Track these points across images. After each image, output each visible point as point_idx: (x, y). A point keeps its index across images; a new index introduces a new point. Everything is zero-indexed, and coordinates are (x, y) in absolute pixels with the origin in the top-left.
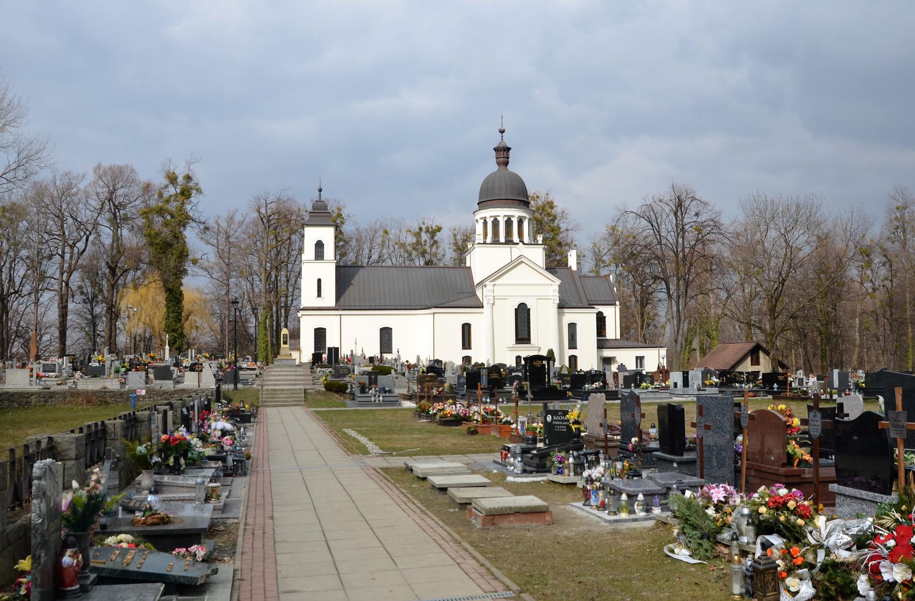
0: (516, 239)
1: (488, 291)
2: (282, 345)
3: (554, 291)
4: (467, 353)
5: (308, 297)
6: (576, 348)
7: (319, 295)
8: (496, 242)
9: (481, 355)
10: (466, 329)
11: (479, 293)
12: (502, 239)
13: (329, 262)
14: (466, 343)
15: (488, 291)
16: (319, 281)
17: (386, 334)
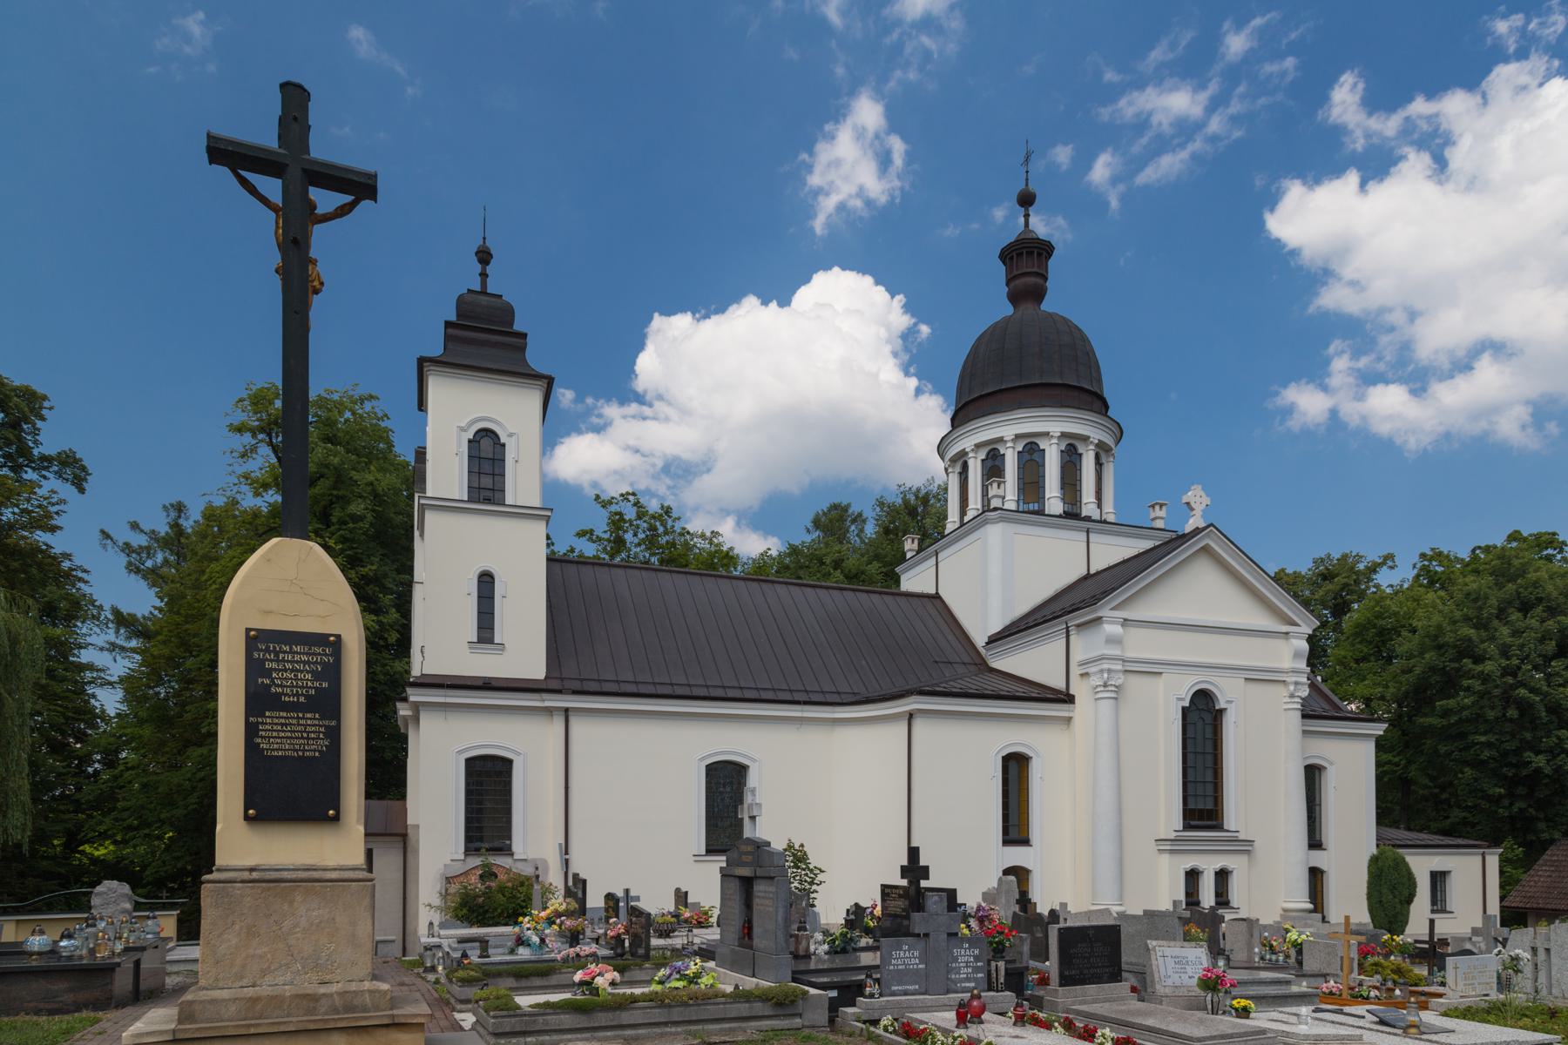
0: (1089, 507)
2: (239, 843)
10: (1015, 767)
12: (1054, 505)
13: (523, 513)
14: (1015, 830)
16: (486, 581)
17: (726, 785)
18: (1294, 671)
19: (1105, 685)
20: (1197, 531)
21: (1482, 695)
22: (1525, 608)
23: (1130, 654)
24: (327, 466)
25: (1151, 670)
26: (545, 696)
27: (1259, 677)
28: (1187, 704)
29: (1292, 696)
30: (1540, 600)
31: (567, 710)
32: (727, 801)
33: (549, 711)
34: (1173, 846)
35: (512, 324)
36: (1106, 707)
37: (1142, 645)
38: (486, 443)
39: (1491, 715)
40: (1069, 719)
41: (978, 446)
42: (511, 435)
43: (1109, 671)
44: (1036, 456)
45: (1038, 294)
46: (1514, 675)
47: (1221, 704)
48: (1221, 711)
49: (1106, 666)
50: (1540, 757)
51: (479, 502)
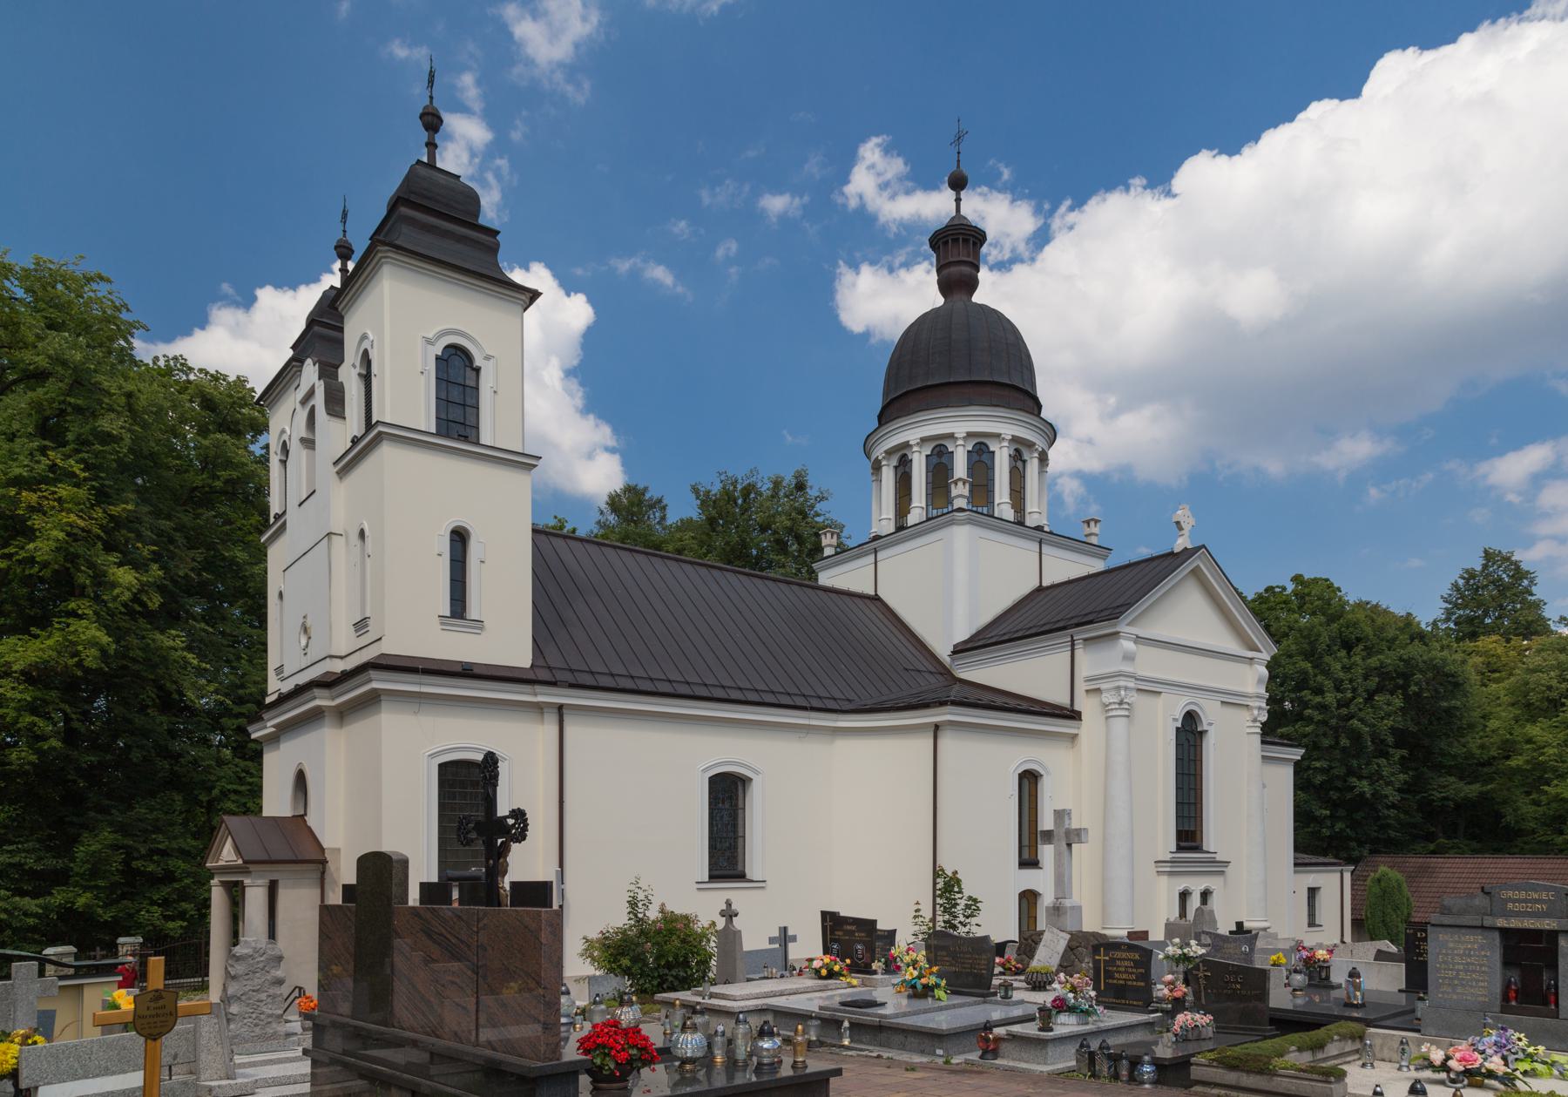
15: (1129, 657)
16: (460, 538)
19: (1121, 703)
20: (1187, 553)
21: (1325, 723)
22: (1348, 646)
23: (1141, 673)
24: (64, 363)
25: (1151, 688)
26: (538, 688)
27: (1232, 701)
29: (1255, 720)
30: (1359, 640)
31: (560, 707)
32: (726, 819)
33: (539, 708)
34: (1171, 868)
35: (477, 216)
36: (1119, 725)
37: (1152, 664)
39: (1326, 742)
40: (1074, 737)
41: (924, 440)
43: (1126, 688)
44: (985, 457)
45: (971, 285)
48: (1202, 733)
49: (1122, 683)
50: (1365, 783)
51: (447, 436)
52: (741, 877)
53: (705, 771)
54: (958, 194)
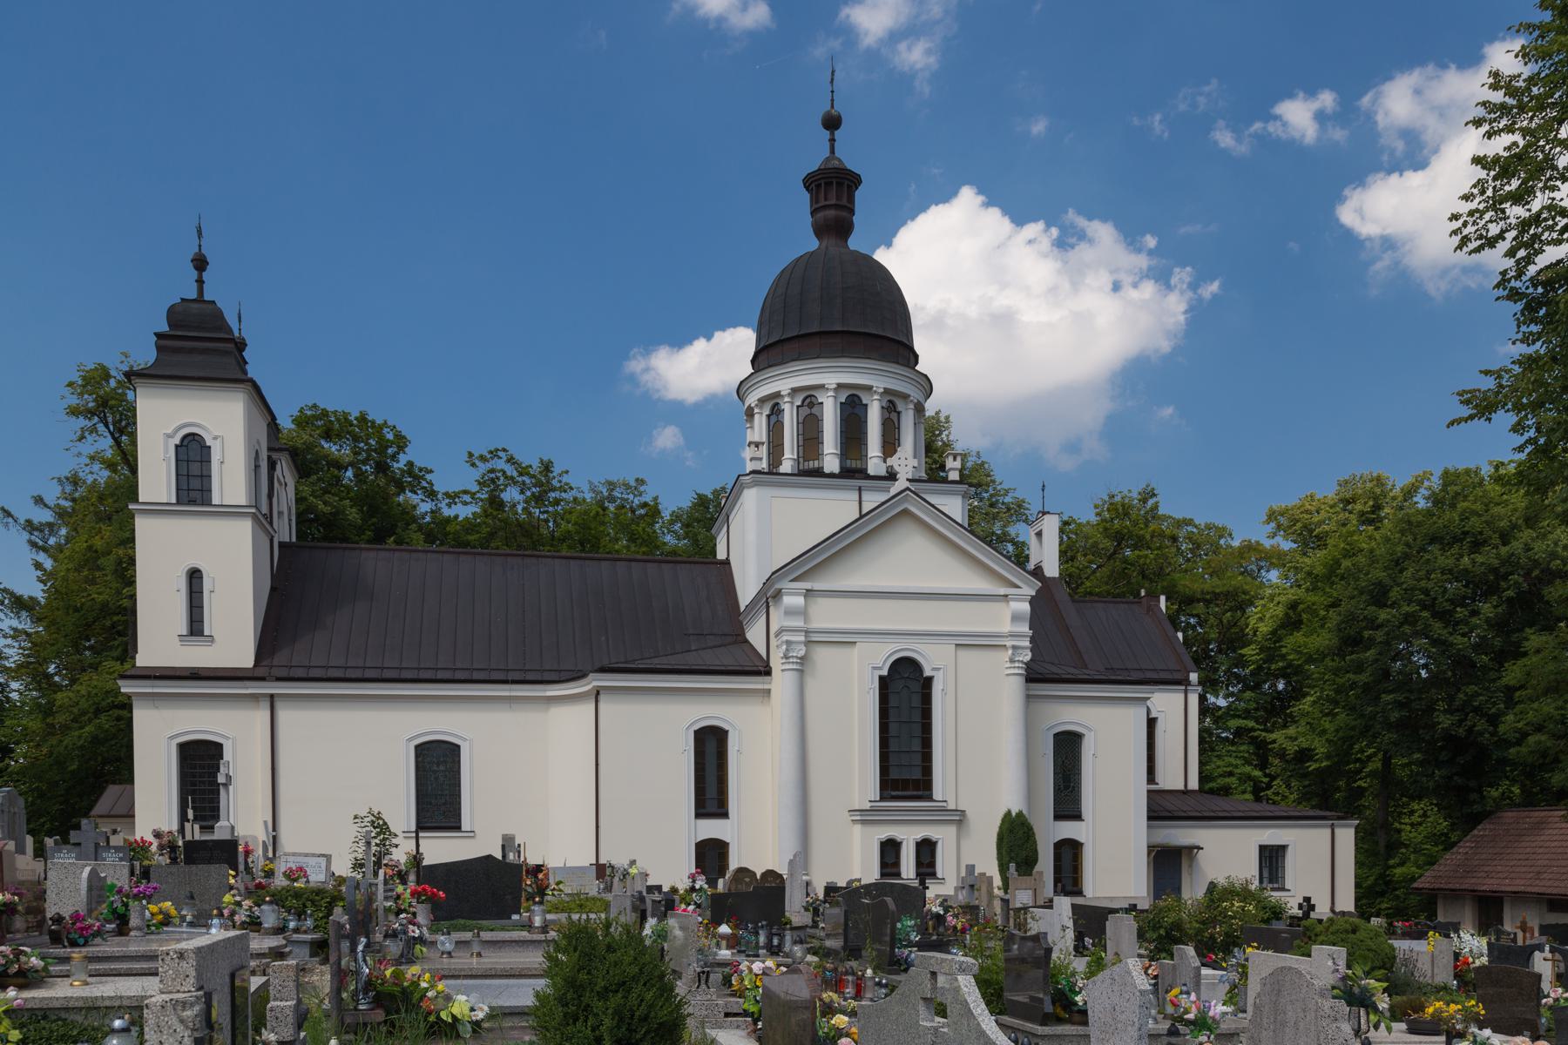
0: (875, 465)
1: (790, 612)
3: (1016, 618)
4: (711, 829)
5: (159, 639)
6: (1077, 817)
7: (196, 627)
8: (810, 473)
9: (758, 840)
11: (755, 635)
12: (831, 464)
15: (790, 612)
16: (194, 576)
18: (1013, 635)
23: (816, 624)
25: (844, 640)
28: (885, 672)
29: (1012, 661)
31: (272, 696)
37: (828, 615)
38: (194, 445)
40: (769, 691)
42: (215, 438)
43: (788, 643)
46: (1414, 624)
47: (927, 673)
48: (930, 680)
52: (457, 827)
53: (410, 740)
54: (832, 134)
